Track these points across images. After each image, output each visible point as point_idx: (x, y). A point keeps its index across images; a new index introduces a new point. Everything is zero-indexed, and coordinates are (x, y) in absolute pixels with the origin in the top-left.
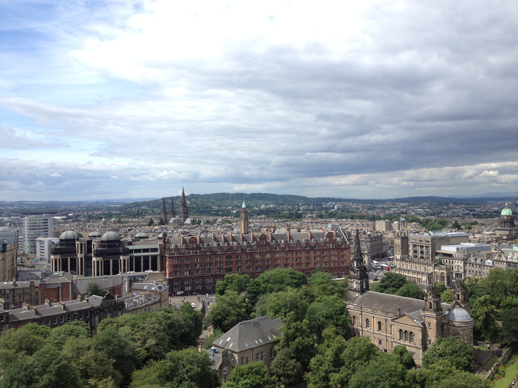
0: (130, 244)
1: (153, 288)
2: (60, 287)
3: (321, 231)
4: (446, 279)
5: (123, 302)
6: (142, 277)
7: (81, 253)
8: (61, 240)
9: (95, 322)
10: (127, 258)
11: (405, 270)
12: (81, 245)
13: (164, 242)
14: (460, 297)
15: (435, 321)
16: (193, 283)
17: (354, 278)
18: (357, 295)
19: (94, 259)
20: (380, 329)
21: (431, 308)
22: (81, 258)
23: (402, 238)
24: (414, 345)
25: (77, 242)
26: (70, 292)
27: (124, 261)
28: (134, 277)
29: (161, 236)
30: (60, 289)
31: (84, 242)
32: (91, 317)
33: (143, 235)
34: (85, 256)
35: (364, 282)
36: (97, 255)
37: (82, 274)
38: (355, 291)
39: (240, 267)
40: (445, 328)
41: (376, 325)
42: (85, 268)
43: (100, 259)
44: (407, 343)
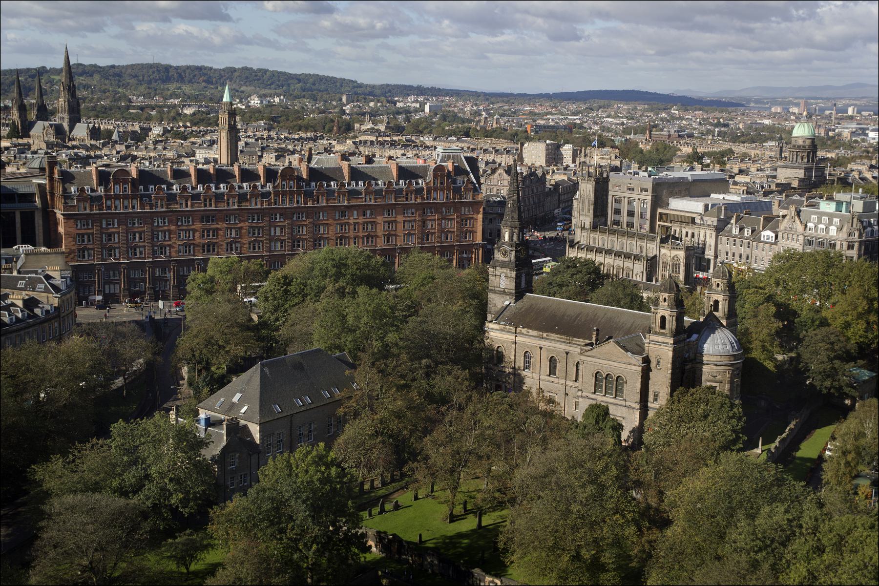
3: (420, 162)
4: (682, 268)
11: (599, 251)
14: (720, 307)
15: (671, 354)
17: (503, 265)
18: (507, 303)
20: (552, 371)
21: (663, 326)
23: (597, 181)
24: (623, 403)
35: (523, 275)
38: (503, 293)
40: (688, 367)
41: (546, 365)
44: (609, 399)
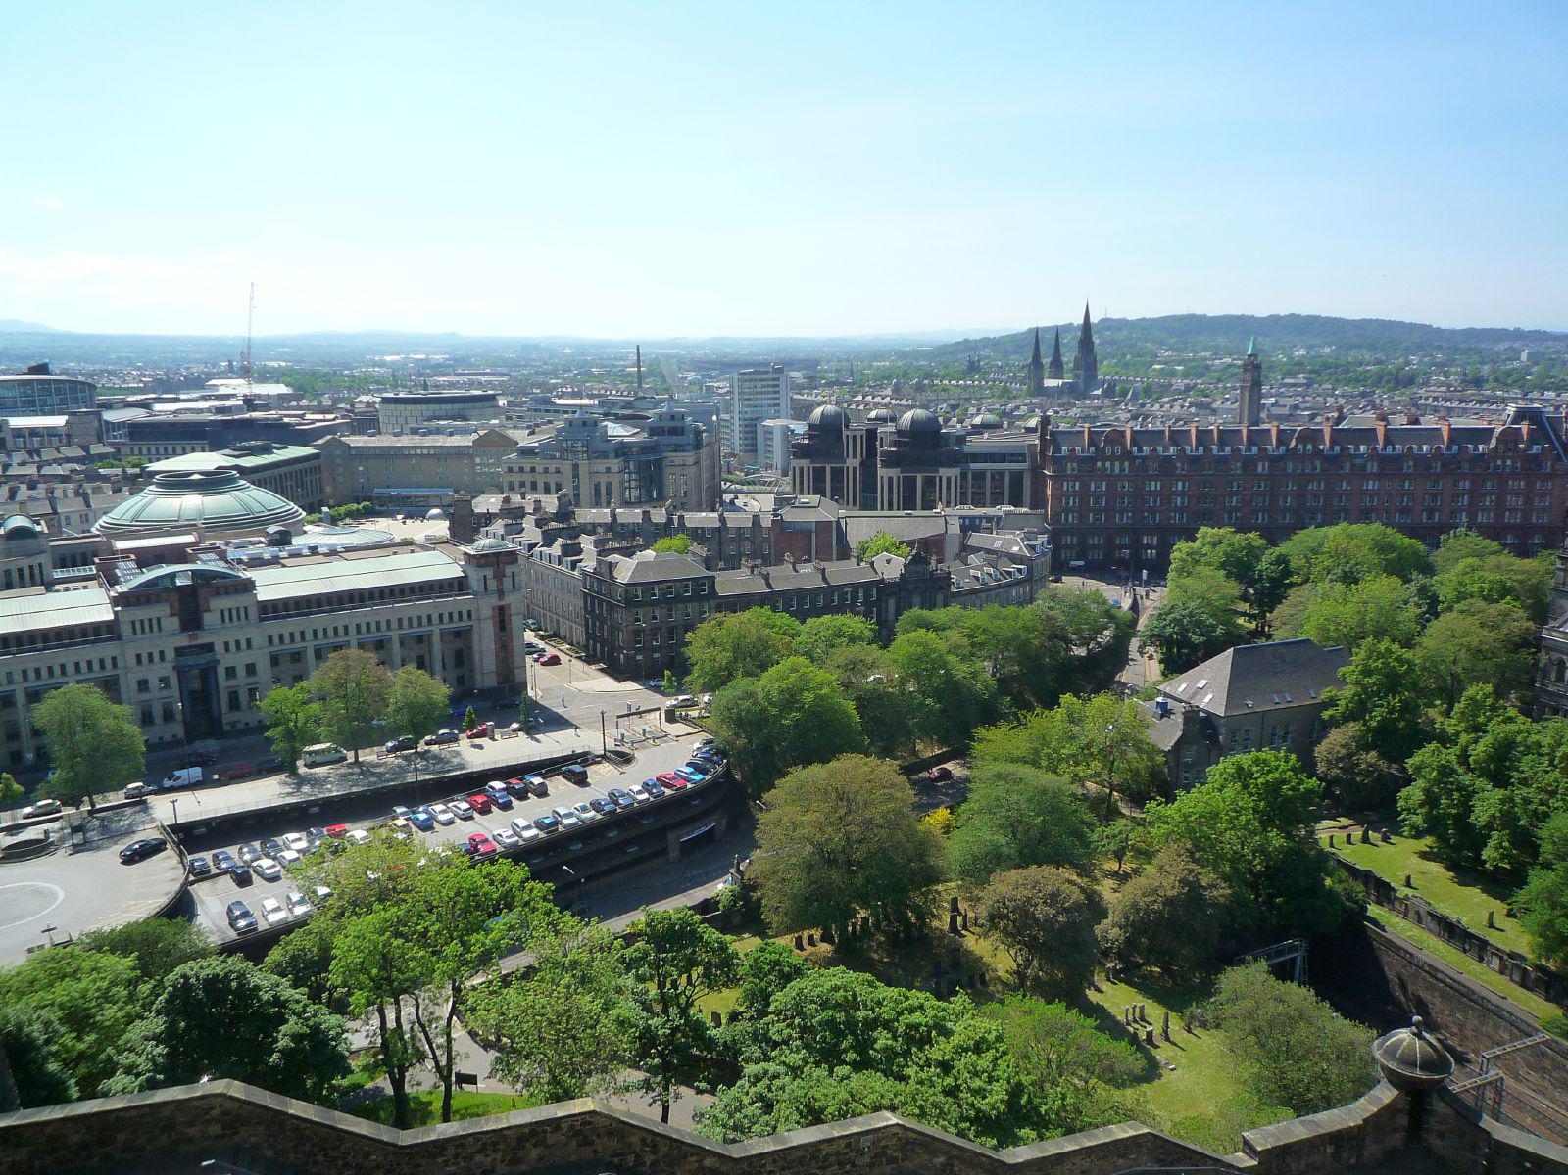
0: (961, 440)
1: (1016, 549)
2: (814, 529)
5: (949, 573)
6: (989, 519)
7: (855, 457)
8: (812, 427)
9: (887, 612)
10: (953, 472)
12: (854, 437)
13: (1042, 438)
16: (1110, 541)
19: (883, 472)
22: (855, 469)
25: (845, 433)
26: (834, 542)
27: (949, 479)
28: (973, 518)
29: (1033, 423)
30: (814, 535)
31: (859, 434)
32: (879, 599)
33: (990, 418)
34: (861, 464)
36: (886, 464)
37: (855, 504)
39: (1236, 509)
42: (863, 490)
43: (894, 472)
